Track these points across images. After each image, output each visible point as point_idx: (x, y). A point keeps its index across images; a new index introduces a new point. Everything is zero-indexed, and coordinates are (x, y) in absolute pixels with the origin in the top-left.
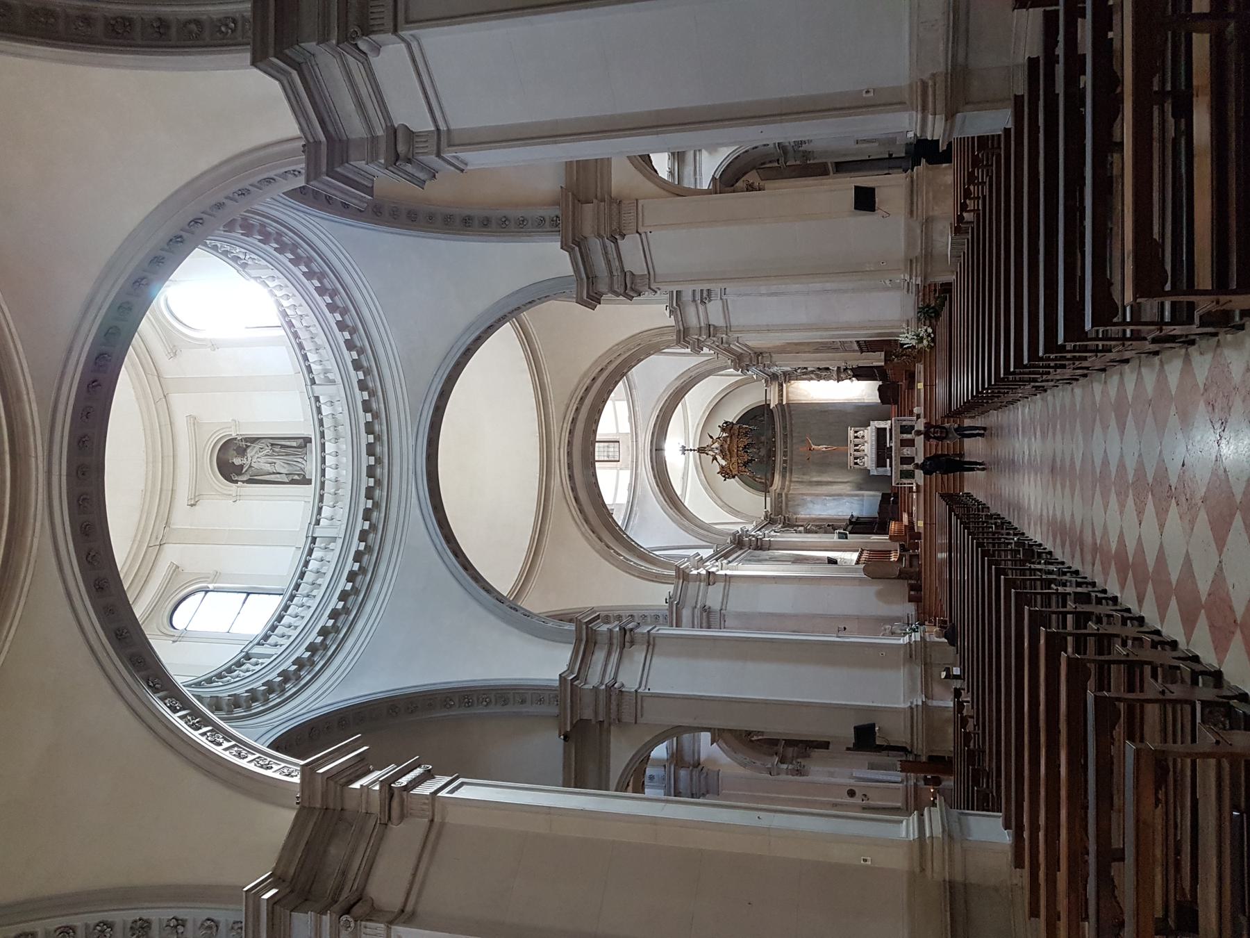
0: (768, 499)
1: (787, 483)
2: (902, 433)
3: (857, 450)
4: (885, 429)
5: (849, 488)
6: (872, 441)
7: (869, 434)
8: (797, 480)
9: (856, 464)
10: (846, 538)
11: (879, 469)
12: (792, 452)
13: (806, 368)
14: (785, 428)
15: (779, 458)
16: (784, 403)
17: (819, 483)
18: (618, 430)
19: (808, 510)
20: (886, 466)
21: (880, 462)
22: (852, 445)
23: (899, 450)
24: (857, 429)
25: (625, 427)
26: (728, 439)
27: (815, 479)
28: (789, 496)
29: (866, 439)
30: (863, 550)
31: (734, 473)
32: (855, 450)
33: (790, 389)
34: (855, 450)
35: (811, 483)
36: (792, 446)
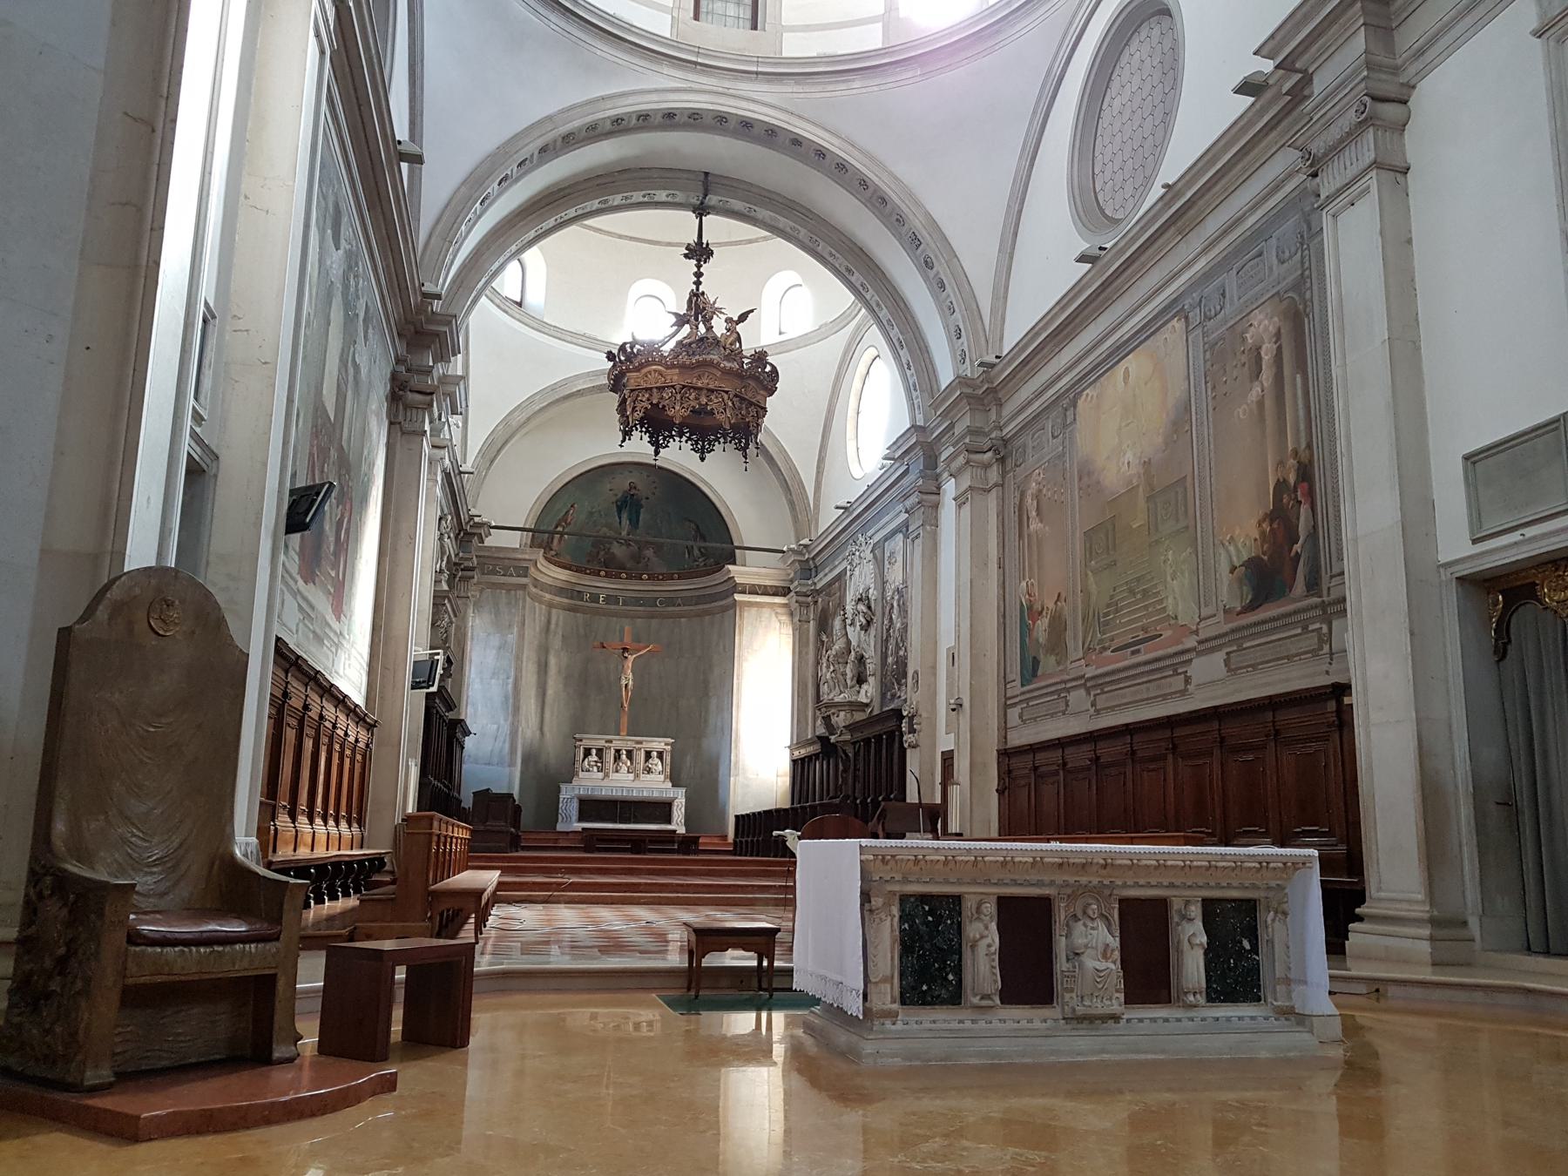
0: (512, 540)
1: (548, 596)
2: (1210, 908)
3: (617, 757)
4: (669, 821)
5: (529, 733)
6: (641, 790)
7: (654, 784)
8: (553, 621)
9: (587, 752)
10: (415, 686)
11: (575, 804)
12: (616, 615)
14: (670, 602)
15: (603, 585)
16: (738, 597)
17: (543, 668)
18: (793, 29)
19: (483, 635)
20: (581, 819)
21: (591, 807)
22: (630, 745)
23: (1097, 892)
24: (667, 757)
25: (795, 47)
26: (735, 366)
27: (552, 661)
28: (520, 593)
29: (645, 777)
30: (370, 727)
31: (633, 380)
32: (618, 751)
33: (766, 612)
34: (618, 751)
35: (543, 651)
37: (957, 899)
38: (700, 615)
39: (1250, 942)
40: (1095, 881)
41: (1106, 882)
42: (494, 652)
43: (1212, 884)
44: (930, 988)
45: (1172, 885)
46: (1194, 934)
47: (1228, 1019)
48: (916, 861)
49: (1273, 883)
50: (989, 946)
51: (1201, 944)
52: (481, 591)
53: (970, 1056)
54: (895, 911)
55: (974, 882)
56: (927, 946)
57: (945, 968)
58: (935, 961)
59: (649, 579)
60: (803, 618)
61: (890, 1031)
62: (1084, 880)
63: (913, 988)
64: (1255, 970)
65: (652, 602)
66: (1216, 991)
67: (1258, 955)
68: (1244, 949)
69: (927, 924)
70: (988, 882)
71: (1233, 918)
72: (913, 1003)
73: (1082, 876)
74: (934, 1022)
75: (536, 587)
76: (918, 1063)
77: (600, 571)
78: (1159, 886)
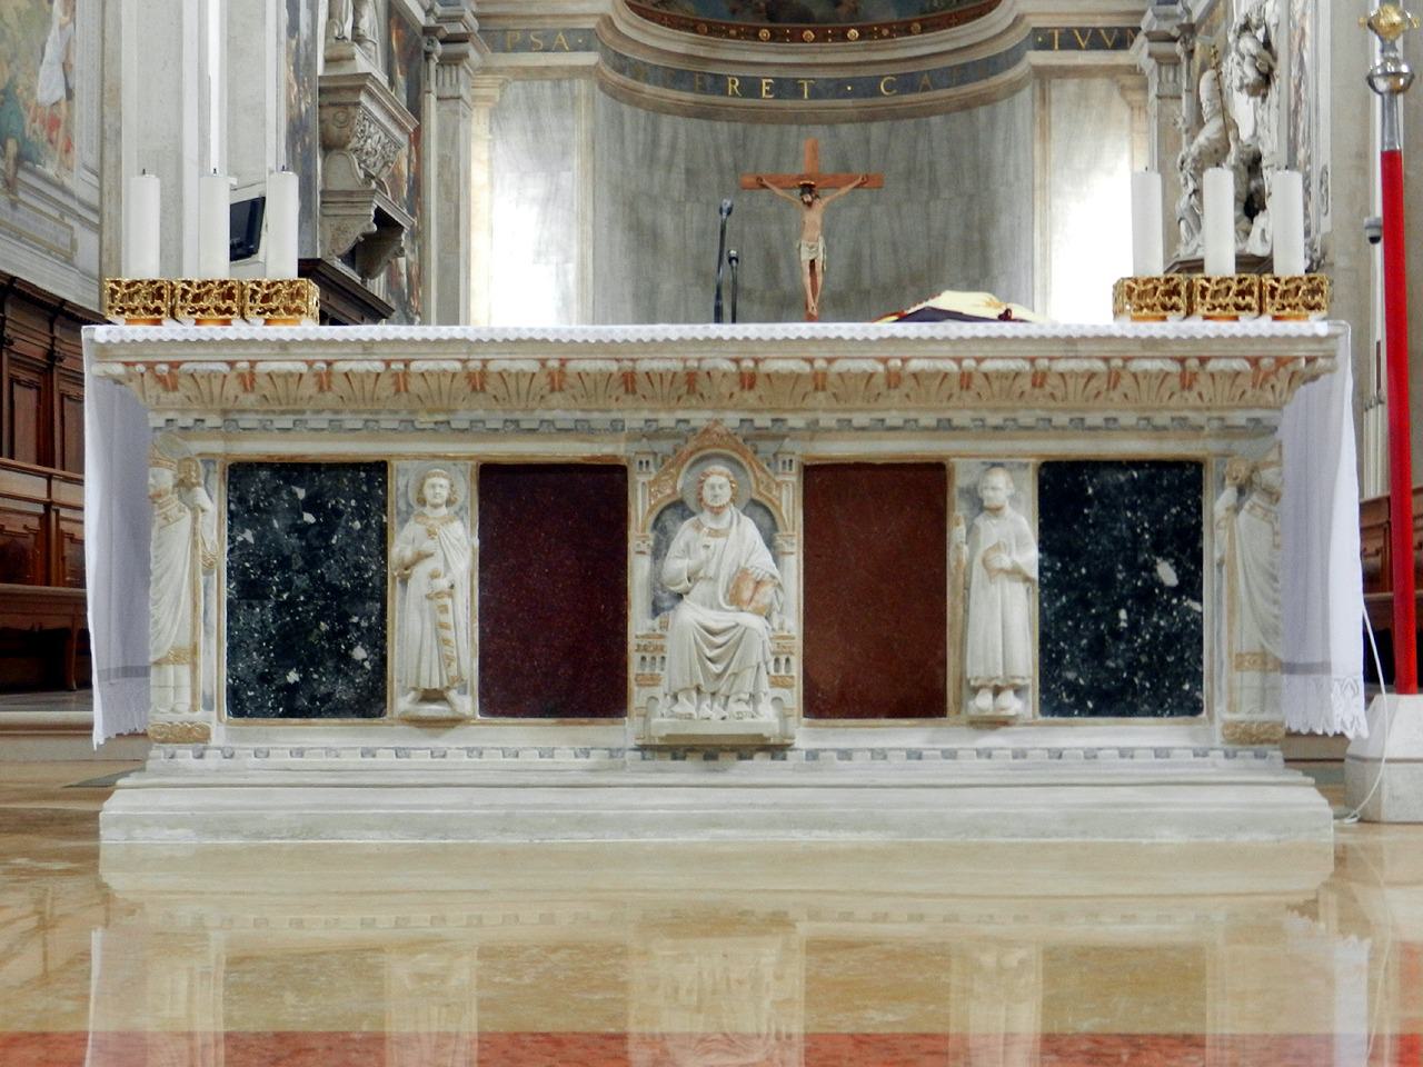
1: (649, 89)
8: (665, 137)
12: (798, 119)
13: (1265, 81)
14: (907, 83)
33: (1099, 86)
36: (817, 119)
37: (379, 469)
38: (967, 106)
39: (1178, 566)
40: (731, 419)
41: (763, 420)
42: (536, 209)
43: (1061, 419)
44: (306, 679)
45: (945, 427)
46: (997, 547)
47: (1091, 755)
48: (248, 381)
49: (1239, 418)
50: (434, 576)
51: (1015, 573)
52: (503, 86)
53: (369, 828)
54: (212, 503)
55: (410, 428)
56: (302, 581)
57: (344, 633)
58: (318, 619)
59: (860, 38)
60: (1169, 89)
61: (187, 772)
62: (700, 418)
63: (264, 679)
64: (1188, 638)
65: (869, 88)
66: (1072, 688)
67: (1200, 600)
68: (1161, 585)
69: (302, 530)
70: (443, 429)
71: (1134, 508)
72: (260, 712)
73: (698, 409)
74: (300, 752)
75: (621, 70)
76: (234, 841)
77: (758, 29)
78: (909, 427)
